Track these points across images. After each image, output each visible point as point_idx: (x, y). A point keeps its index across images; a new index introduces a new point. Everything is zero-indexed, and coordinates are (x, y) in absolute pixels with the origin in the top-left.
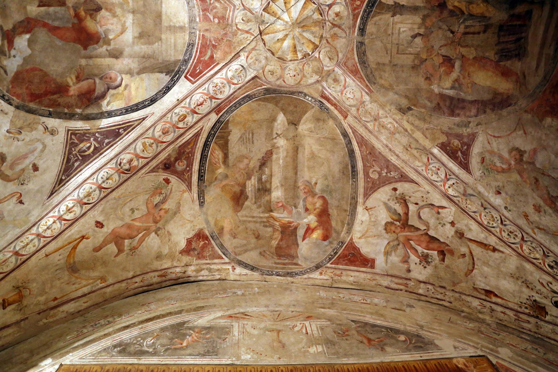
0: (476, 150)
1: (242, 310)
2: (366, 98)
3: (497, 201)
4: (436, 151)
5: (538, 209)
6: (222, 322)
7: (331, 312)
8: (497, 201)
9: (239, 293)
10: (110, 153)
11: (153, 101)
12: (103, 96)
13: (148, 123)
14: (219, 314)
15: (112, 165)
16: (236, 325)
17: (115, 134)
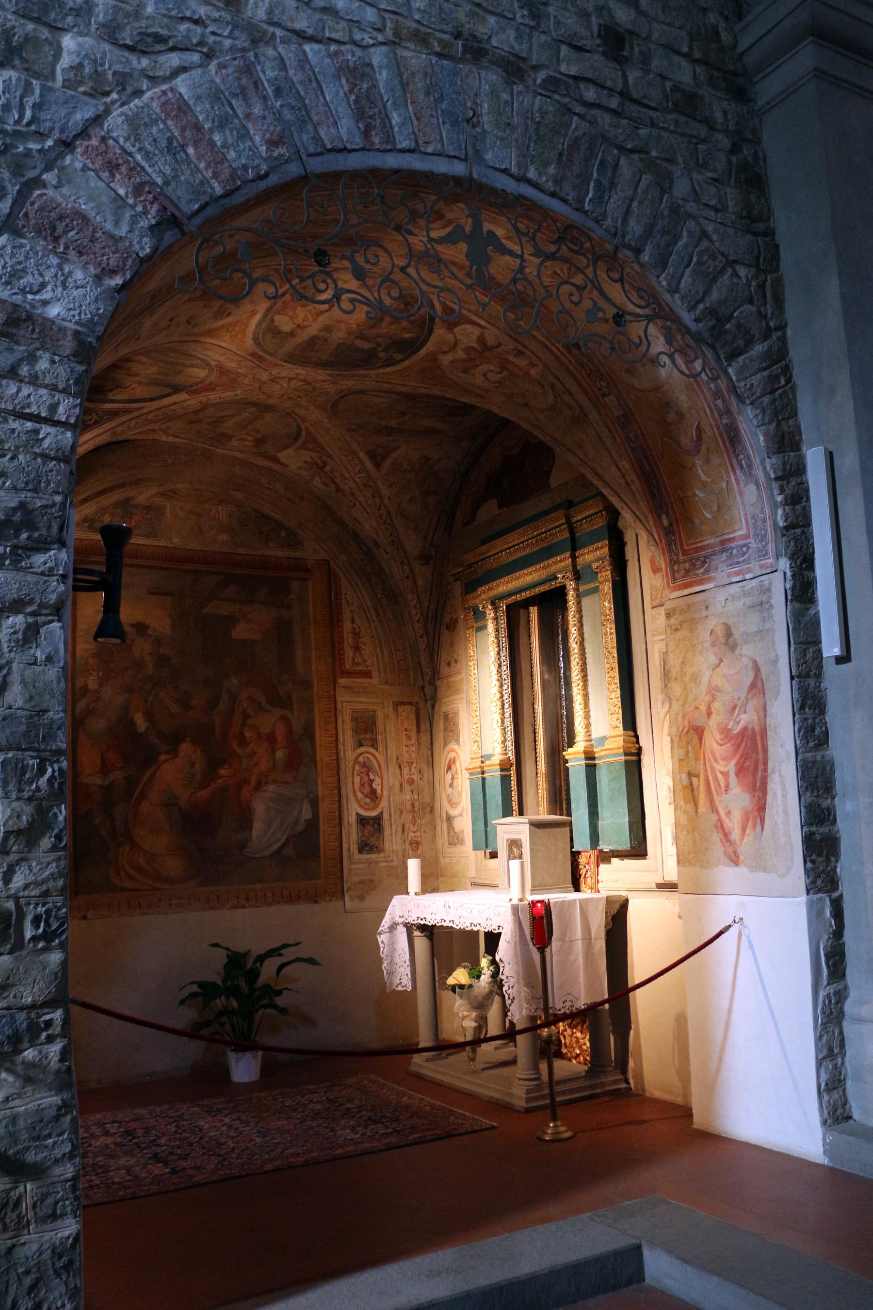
0: (394, 455)
1: (172, 487)
2: (326, 420)
3: (385, 491)
4: (361, 454)
5: (411, 500)
6: (158, 500)
7: (240, 496)
8: (385, 491)
9: (170, 461)
10: (108, 426)
11: (152, 400)
12: (111, 390)
13: (144, 411)
14: (155, 490)
15: (109, 433)
16: (168, 504)
17: (115, 414)
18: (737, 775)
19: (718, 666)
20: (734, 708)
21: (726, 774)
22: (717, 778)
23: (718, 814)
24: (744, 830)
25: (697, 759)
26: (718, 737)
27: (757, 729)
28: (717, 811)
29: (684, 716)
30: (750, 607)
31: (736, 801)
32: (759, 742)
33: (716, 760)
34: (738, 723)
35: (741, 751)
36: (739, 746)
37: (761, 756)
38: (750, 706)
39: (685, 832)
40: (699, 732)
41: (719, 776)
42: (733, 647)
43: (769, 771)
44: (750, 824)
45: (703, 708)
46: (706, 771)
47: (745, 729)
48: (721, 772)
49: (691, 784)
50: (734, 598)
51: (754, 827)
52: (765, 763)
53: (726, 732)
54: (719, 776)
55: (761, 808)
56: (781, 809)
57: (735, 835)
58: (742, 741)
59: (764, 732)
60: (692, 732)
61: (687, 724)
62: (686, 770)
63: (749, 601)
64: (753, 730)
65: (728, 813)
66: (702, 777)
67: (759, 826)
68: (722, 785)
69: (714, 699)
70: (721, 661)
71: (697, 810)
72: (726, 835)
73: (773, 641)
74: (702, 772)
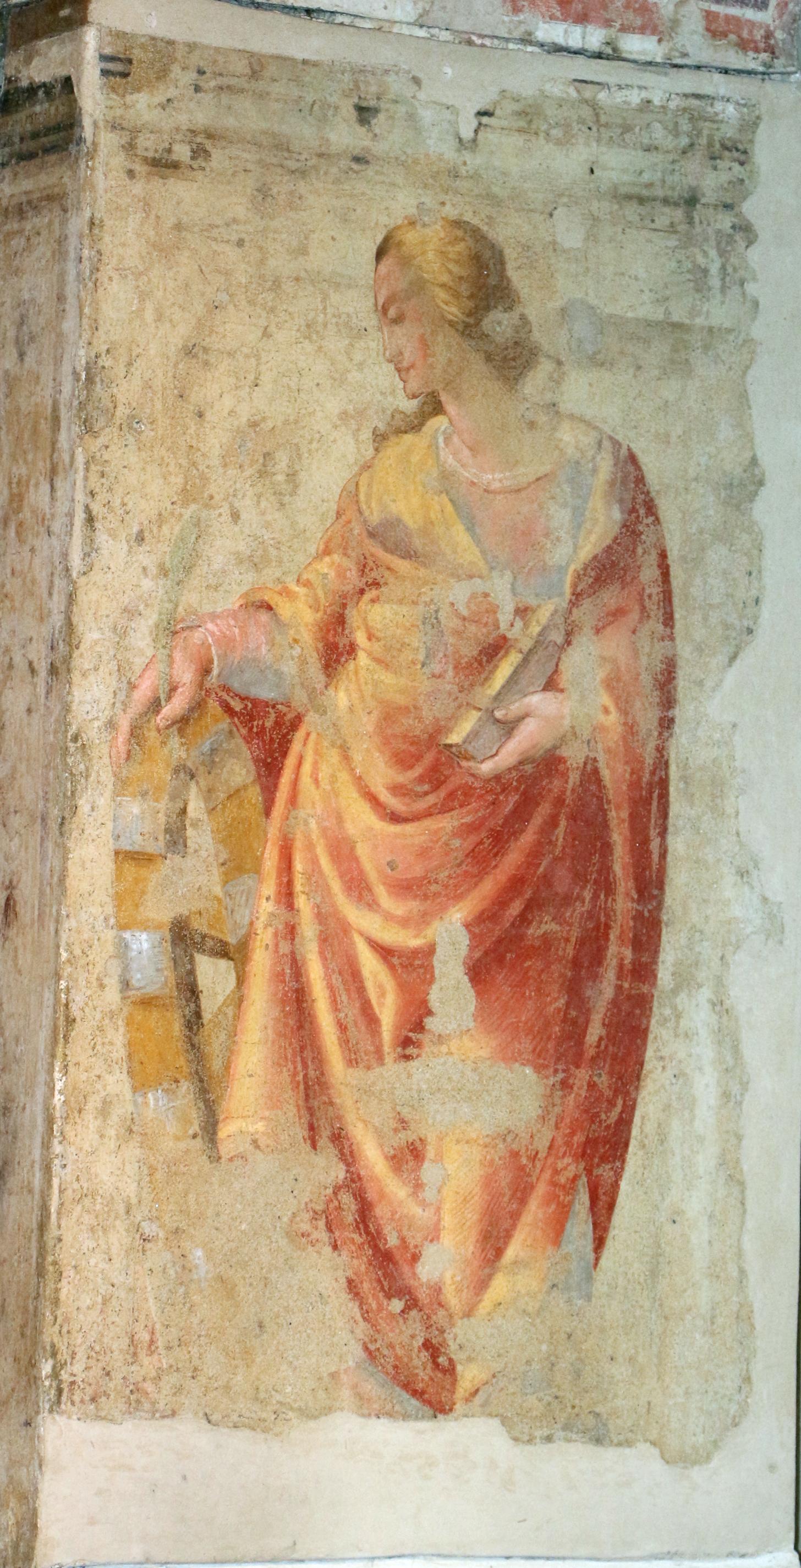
18: (478, 973)
19: (415, 425)
20: (494, 650)
21: (412, 967)
22: (354, 976)
23: (348, 1156)
24: (493, 1242)
25: (238, 865)
26: (381, 775)
27: (613, 776)
28: (338, 1138)
29: (172, 629)
30: (623, 197)
31: (469, 1094)
32: (619, 838)
33: (358, 887)
34: (509, 727)
35: (513, 859)
36: (500, 839)
37: (623, 904)
38: (585, 661)
39: (118, 1238)
40: (269, 734)
41: (370, 964)
42: (512, 361)
43: (665, 974)
44: (535, 1211)
45: (302, 615)
46: (291, 931)
47: (550, 763)
48: (385, 952)
49: (190, 990)
50: (529, 116)
51: (557, 1228)
52: (647, 935)
53: (430, 766)
54: (370, 964)
55: (599, 1144)
56: (705, 1160)
57: (441, 1264)
58: (521, 813)
59: (651, 796)
60: (217, 725)
61: (186, 675)
62: (161, 910)
63: (619, 165)
64: (591, 774)
65: (410, 1156)
66: (261, 962)
67: (580, 1226)
68: (388, 1013)
69: (370, 582)
70: (433, 406)
71: (210, 1128)
72: (385, 1267)
73: (743, 399)
74: (264, 936)
